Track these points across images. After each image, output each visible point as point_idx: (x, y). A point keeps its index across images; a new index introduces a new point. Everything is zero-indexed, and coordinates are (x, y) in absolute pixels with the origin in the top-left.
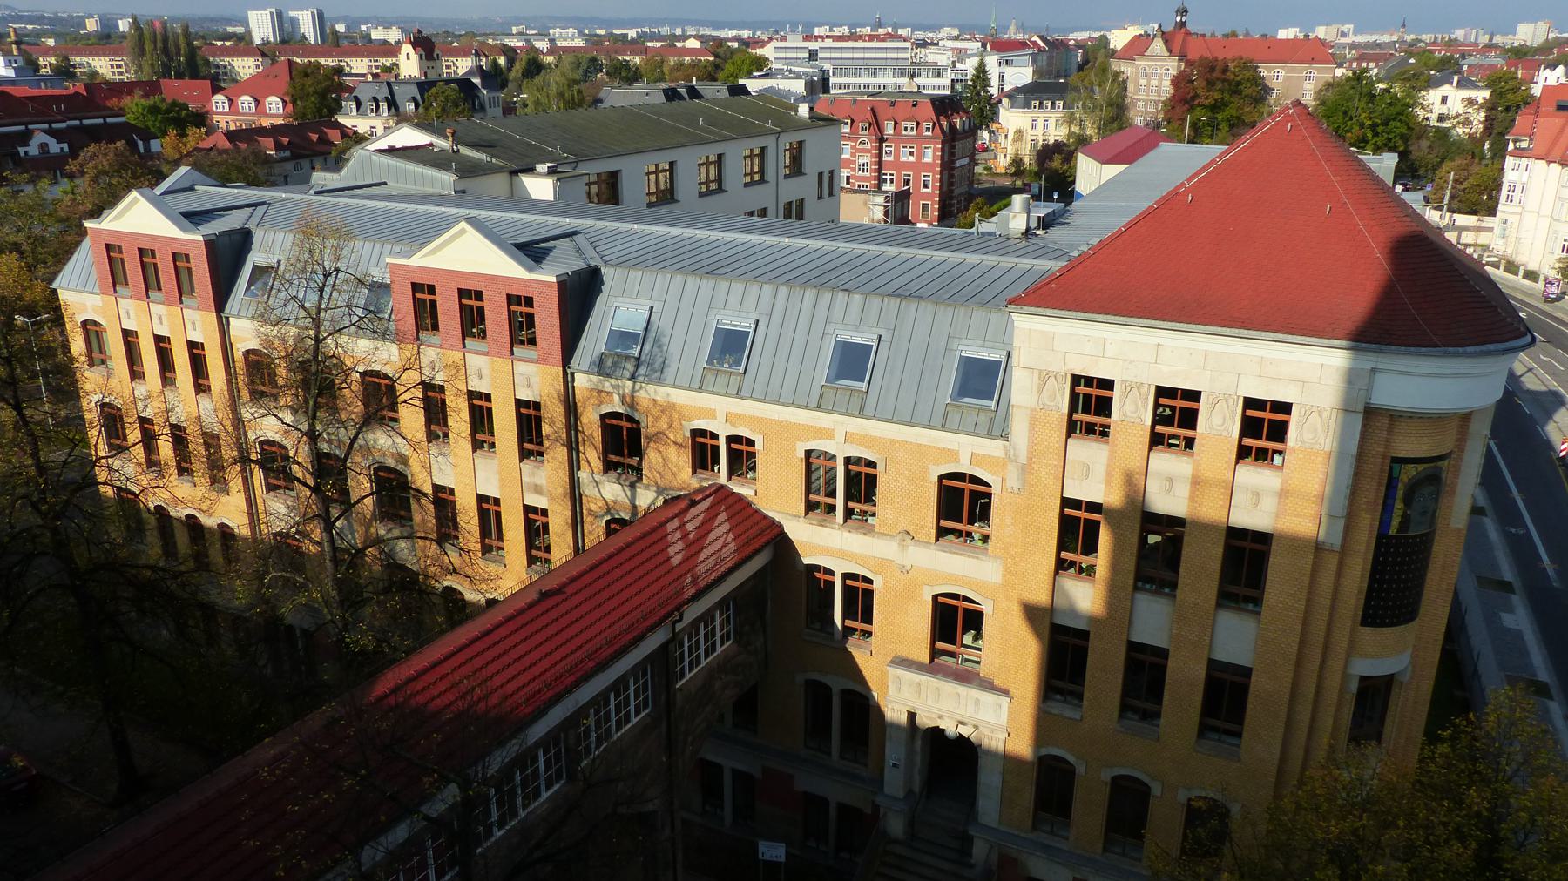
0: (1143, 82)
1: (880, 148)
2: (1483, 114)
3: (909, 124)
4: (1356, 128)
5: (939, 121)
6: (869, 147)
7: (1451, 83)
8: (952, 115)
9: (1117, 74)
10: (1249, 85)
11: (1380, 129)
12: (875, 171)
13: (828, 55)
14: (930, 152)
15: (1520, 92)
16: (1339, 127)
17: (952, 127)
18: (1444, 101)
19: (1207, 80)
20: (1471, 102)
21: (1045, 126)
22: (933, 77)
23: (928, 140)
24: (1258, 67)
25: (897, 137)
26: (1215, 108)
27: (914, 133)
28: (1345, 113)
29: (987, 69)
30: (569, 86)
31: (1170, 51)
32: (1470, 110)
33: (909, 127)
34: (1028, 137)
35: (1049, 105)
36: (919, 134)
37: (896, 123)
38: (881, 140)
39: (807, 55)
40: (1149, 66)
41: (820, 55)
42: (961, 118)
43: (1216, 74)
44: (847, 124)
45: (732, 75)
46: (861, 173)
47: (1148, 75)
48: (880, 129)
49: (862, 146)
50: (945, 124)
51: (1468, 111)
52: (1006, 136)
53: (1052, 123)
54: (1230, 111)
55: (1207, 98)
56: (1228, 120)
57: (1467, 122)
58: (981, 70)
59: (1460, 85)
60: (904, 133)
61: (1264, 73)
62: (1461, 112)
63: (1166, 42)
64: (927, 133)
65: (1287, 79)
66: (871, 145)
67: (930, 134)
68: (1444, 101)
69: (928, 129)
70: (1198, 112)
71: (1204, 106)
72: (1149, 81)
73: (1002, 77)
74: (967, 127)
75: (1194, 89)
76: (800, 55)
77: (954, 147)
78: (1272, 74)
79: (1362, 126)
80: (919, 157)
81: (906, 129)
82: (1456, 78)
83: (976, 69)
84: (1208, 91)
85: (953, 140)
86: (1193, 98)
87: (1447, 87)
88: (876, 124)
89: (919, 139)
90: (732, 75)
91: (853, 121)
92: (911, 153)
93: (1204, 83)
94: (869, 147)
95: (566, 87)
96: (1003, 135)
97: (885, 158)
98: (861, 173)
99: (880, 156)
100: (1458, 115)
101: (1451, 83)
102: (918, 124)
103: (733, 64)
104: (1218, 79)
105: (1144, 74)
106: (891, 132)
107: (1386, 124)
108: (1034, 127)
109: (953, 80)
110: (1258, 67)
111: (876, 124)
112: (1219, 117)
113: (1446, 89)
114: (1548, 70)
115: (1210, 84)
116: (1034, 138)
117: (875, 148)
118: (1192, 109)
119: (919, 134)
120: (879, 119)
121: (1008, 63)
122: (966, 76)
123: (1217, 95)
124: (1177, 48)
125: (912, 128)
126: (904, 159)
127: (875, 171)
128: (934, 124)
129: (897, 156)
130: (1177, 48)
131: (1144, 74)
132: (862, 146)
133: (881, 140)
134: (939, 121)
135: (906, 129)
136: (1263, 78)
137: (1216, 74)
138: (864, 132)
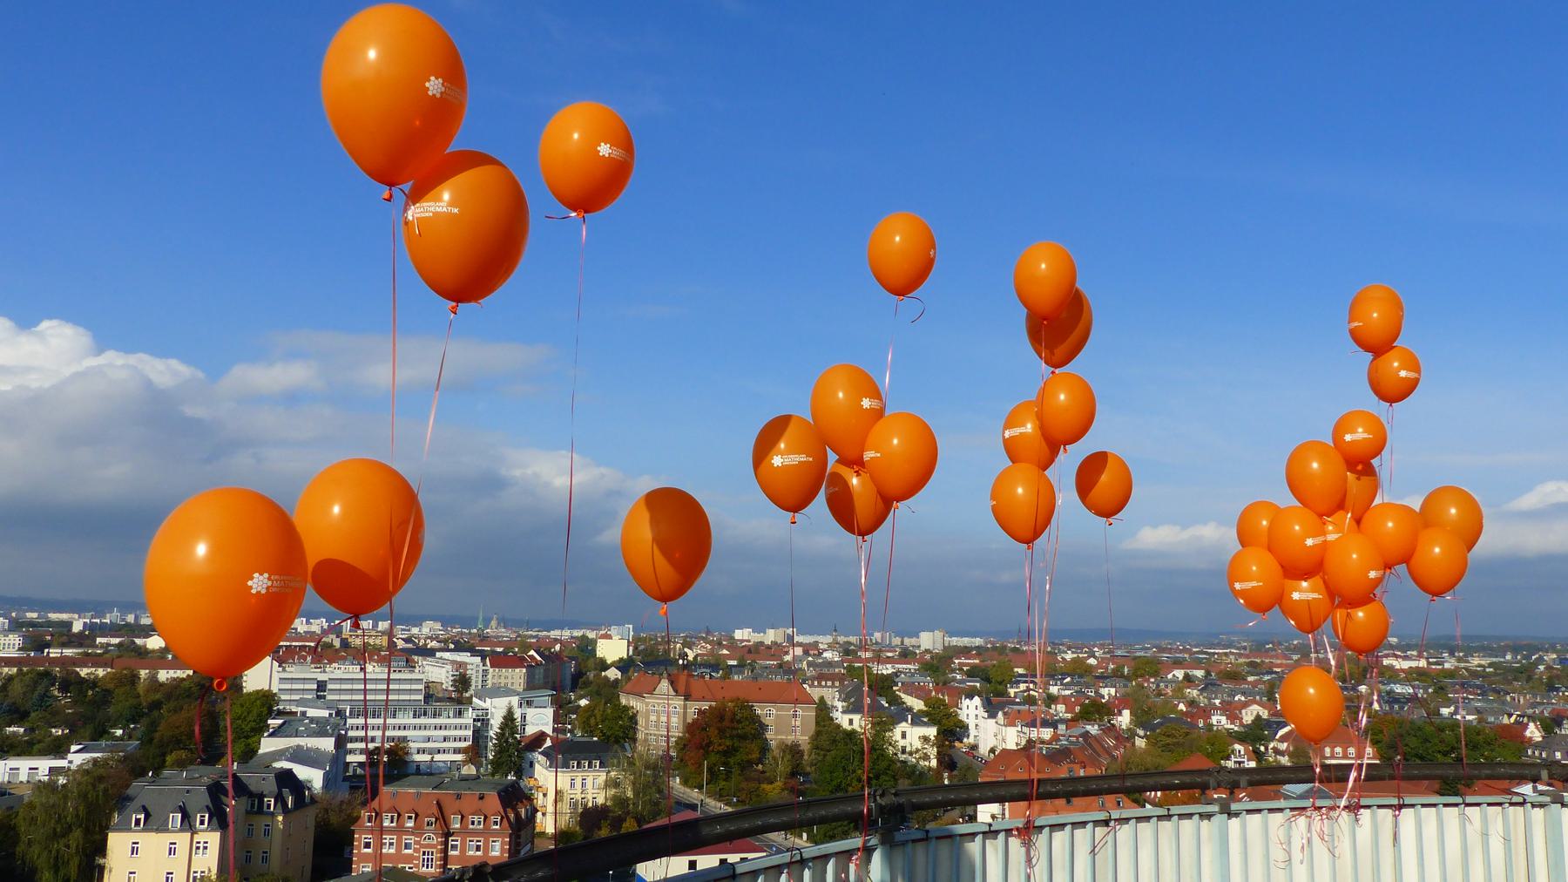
0: (653, 718)
1: (446, 843)
2: (935, 749)
3: (476, 819)
4: (855, 783)
5: (506, 814)
6: (435, 842)
7: (907, 721)
8: (517, 804)
9: (626, 708)
10: (748, 723)
11: (874, 782)
12: (440, 866)
13: (338, 687)
14: (498, 844)
15: (952, 718)
16: (841, 782)
17: (518, 815)
18: (904, 736)
19: (719, 729)
20: (925, 739)
21: (583, 785)
22: (455, 717)
23: (496, 834)
24: (753, 706)
25: (465, 832)
26: (728, 753)
27: (482, 826)
28: (844, 769)
29: (515, 717)
30: (94, 786)
31: (676, 691)
32: (926, 746)
33: (476, 820)
34: (566, 798)
35: (587, 764)
36: (487, 827)
37: (463, 817)
38: (447, 834)
39: (315, 687)
40: (659, 704)
41: (330, 686)
42: (525, 808)
43: (726, 723)
44: (410, 818)
45: (239, 718)
46: (424, 869)
47: (657, 712)
48: (446, 823)
49: (427, 842)
50: (512, 816)
51: (926, 746)
52: (545, 795)
53: (589, 782)
54: (739, 757)
55: (720, 745)
56: (739, 764)
57: (926, 757)
58: (509, 718)
59: (914, 723)
60: (471, 827)
61: (759, 712)
62: (920, 748)
63: (672, 683)
64: (495, 827)
65: (777, 716)
66: (436, 840)
67: (498, 827)
68: (904, 736)
69: (496, 823)
70: (714, 758)
71: (718, 752)
72: (658, 717)
73: (524, 717)
74: (529, 813)
75: (708, 736)
76: (307, 686)
77: (519, 837)
78: (765, 712)
79: (859, 780)
80: (486, 851)
81: (473, 823)
82: (910, 717)
83: (505, 718)
84: (721, 739)
85: (519, 830)
86: (708, 745)
87: (904, 724)
88: (442, 819)
89: (486, 833)
90: (239, 718)
91: (417, 815)
92: (478, 848)
93: (716, 732)
94: (435, 842)
95: (90, 787)
96: (541, 795)
97: (452, 853)
98: (424, 869)
99: (445, 851)
100: (917, 751)
101: (907, 721)
102: (486, 818)
103: (242, 706)
104: (728, 728)
105: (653, 711)
106: (458, 826)
107: (877, 777)
108: (572, 785)
109: (474, 720)
110: (753, 706)
111: (442, 819)
112: (732, 761)
114: (968, 700)
115: (721, 731)
116: (572, 796)
117: (441, 843)
118: (706, 755)
119: (487, 827)
120: (445, 814)
121: (529, 704)
122: (487, 714)
123: (728, 743)
124: (682, 688)
125: (479, 822)
126: (471, 853)
127: (440, 866)
128: (501, 820)
129: (463, 851)
130: (682, 687)
131: (653, 711)
132: (427, 842)
133: (447, 834)
134: (506, 814)
135: (473, 823)
136: (758, 716)
137: (726, 723)
138: (429, 828)
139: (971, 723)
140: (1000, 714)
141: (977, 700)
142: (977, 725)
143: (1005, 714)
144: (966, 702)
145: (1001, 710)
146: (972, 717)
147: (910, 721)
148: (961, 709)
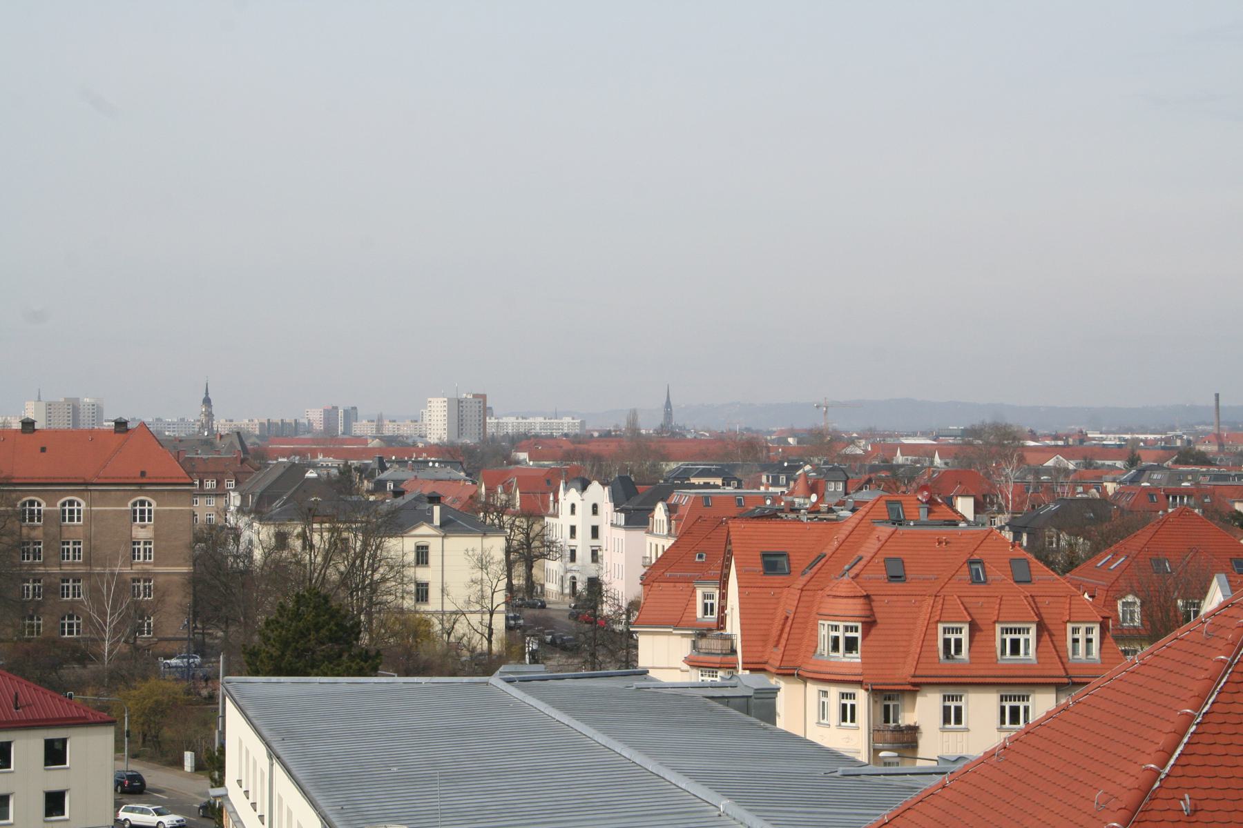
7: (430, 520)
18: (422, 556)
59: (449, 526)
65: (91, 517)
87: (424, 529)
101: (430, 520)
113: (424, 533)
114: (573, 491)
139: (583, 543)
140: (660, 512)
141: (598, 493)
142: (594, 553)
143: (671, 510)
144: (568, 496)
145: (663, 500)
146: (583, 533)
147: (437, 522)
148: (556, 515)
